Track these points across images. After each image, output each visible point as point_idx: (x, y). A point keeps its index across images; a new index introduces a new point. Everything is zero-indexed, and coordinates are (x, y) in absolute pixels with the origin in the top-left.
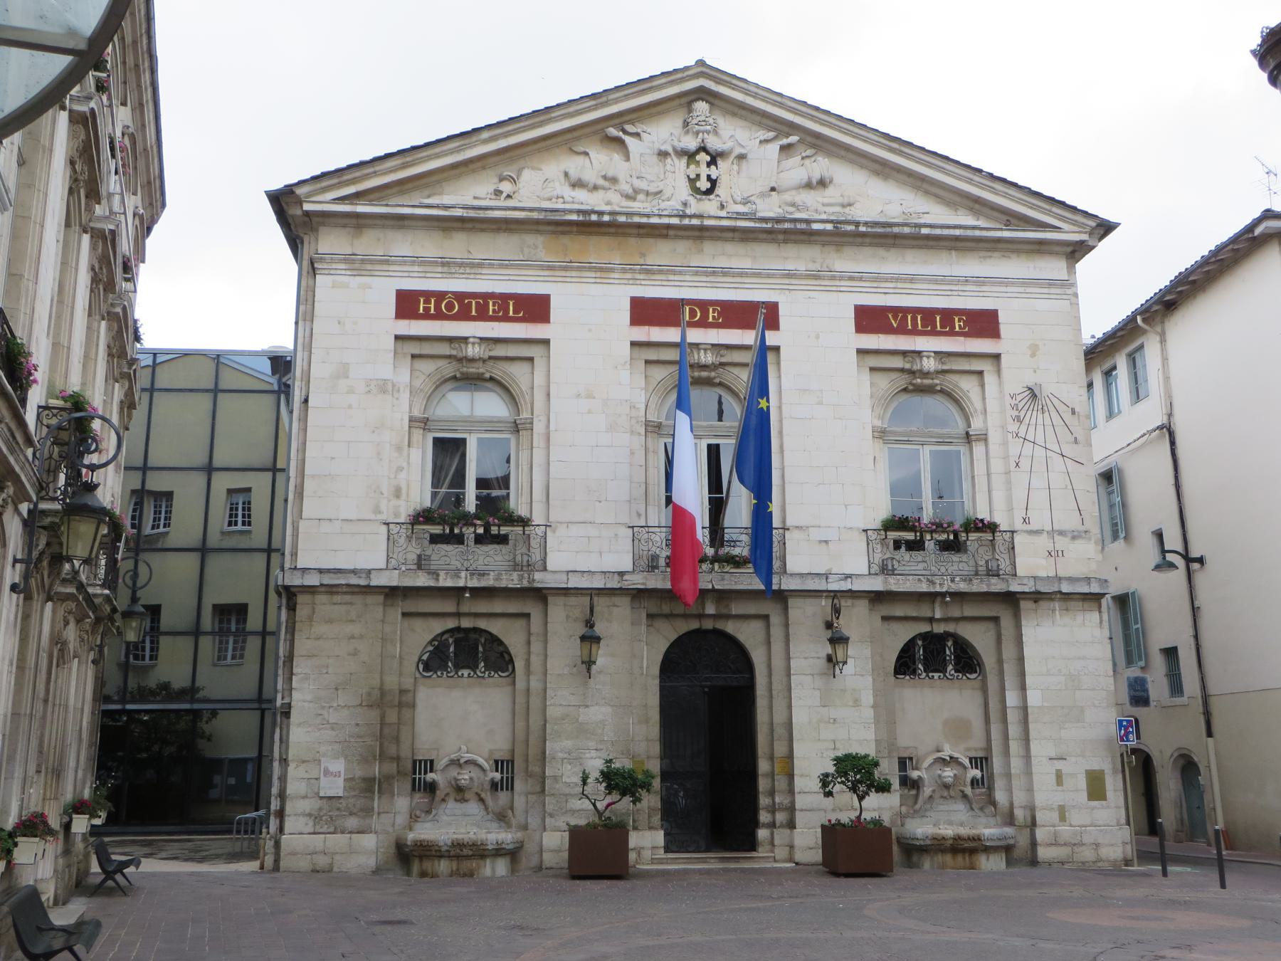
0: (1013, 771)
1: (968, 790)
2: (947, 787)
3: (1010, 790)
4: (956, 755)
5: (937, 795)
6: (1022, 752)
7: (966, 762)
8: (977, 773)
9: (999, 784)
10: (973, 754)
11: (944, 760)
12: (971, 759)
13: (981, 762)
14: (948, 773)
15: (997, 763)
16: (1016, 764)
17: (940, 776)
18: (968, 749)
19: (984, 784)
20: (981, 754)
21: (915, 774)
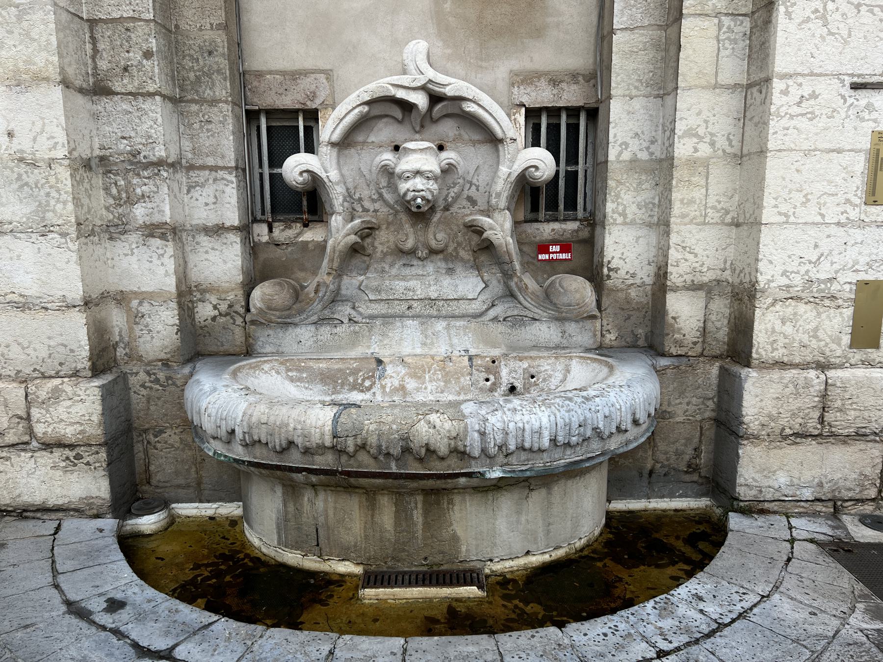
0: (682, 149)
1: (500, 228)
2: (420, 214)
3: (661, 224)
4: (453, 86)
5: (384, 240)
6: (733, 69)
7: (511, 126)
8: (541, 162)
9: (623, 203)
10: (542, 96)
11: (407, 107)
12: (532, 114)
13: (570, 127)
14: (419, 162)
15: (626, 127)
16: (702, 114)
17: (388, 172)
18: (528, 78)
19: (562, 201)
20: (571, 95)
21: (296, 167)
